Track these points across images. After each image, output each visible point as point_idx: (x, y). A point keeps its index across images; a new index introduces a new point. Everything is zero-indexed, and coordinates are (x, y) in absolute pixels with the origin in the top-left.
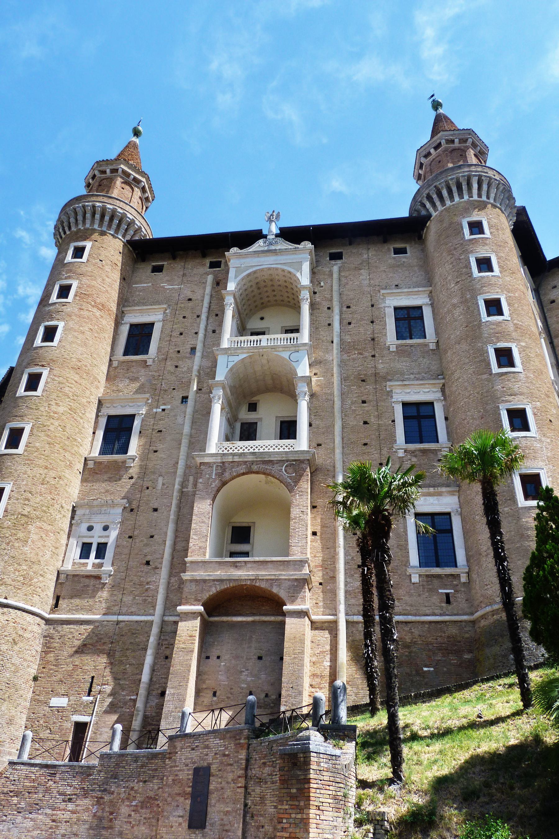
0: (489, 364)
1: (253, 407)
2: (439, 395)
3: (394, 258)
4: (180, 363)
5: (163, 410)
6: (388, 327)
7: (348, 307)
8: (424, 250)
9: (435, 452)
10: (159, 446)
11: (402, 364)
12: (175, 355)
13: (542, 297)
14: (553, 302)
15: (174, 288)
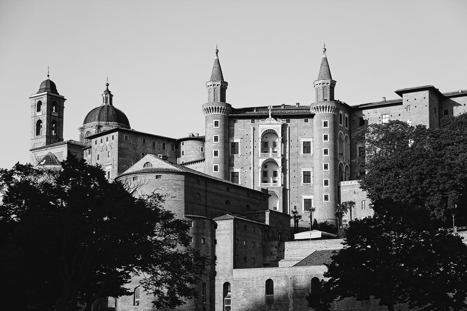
0: (322, 168)
1: (266, 167)
2: (312, 170)
3: (304, 124)
4: (247, 157)
5: (245, 171)
6: (301, 149)
7: (291, 141)
8: (313, 121)
9: (310, 185)
10: (246, 182)
11: (304, 161)
12: (246, 154)
13: (351, 118)
14: (354, 121)
15: (242, 130)
